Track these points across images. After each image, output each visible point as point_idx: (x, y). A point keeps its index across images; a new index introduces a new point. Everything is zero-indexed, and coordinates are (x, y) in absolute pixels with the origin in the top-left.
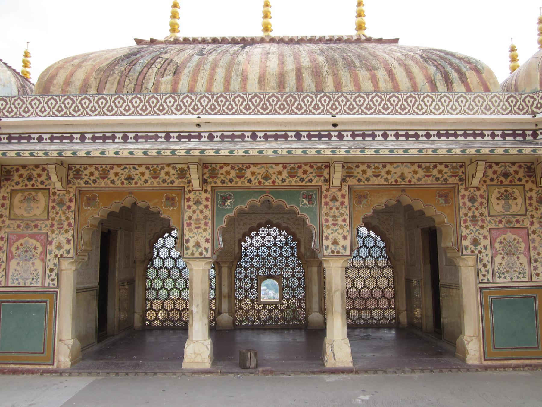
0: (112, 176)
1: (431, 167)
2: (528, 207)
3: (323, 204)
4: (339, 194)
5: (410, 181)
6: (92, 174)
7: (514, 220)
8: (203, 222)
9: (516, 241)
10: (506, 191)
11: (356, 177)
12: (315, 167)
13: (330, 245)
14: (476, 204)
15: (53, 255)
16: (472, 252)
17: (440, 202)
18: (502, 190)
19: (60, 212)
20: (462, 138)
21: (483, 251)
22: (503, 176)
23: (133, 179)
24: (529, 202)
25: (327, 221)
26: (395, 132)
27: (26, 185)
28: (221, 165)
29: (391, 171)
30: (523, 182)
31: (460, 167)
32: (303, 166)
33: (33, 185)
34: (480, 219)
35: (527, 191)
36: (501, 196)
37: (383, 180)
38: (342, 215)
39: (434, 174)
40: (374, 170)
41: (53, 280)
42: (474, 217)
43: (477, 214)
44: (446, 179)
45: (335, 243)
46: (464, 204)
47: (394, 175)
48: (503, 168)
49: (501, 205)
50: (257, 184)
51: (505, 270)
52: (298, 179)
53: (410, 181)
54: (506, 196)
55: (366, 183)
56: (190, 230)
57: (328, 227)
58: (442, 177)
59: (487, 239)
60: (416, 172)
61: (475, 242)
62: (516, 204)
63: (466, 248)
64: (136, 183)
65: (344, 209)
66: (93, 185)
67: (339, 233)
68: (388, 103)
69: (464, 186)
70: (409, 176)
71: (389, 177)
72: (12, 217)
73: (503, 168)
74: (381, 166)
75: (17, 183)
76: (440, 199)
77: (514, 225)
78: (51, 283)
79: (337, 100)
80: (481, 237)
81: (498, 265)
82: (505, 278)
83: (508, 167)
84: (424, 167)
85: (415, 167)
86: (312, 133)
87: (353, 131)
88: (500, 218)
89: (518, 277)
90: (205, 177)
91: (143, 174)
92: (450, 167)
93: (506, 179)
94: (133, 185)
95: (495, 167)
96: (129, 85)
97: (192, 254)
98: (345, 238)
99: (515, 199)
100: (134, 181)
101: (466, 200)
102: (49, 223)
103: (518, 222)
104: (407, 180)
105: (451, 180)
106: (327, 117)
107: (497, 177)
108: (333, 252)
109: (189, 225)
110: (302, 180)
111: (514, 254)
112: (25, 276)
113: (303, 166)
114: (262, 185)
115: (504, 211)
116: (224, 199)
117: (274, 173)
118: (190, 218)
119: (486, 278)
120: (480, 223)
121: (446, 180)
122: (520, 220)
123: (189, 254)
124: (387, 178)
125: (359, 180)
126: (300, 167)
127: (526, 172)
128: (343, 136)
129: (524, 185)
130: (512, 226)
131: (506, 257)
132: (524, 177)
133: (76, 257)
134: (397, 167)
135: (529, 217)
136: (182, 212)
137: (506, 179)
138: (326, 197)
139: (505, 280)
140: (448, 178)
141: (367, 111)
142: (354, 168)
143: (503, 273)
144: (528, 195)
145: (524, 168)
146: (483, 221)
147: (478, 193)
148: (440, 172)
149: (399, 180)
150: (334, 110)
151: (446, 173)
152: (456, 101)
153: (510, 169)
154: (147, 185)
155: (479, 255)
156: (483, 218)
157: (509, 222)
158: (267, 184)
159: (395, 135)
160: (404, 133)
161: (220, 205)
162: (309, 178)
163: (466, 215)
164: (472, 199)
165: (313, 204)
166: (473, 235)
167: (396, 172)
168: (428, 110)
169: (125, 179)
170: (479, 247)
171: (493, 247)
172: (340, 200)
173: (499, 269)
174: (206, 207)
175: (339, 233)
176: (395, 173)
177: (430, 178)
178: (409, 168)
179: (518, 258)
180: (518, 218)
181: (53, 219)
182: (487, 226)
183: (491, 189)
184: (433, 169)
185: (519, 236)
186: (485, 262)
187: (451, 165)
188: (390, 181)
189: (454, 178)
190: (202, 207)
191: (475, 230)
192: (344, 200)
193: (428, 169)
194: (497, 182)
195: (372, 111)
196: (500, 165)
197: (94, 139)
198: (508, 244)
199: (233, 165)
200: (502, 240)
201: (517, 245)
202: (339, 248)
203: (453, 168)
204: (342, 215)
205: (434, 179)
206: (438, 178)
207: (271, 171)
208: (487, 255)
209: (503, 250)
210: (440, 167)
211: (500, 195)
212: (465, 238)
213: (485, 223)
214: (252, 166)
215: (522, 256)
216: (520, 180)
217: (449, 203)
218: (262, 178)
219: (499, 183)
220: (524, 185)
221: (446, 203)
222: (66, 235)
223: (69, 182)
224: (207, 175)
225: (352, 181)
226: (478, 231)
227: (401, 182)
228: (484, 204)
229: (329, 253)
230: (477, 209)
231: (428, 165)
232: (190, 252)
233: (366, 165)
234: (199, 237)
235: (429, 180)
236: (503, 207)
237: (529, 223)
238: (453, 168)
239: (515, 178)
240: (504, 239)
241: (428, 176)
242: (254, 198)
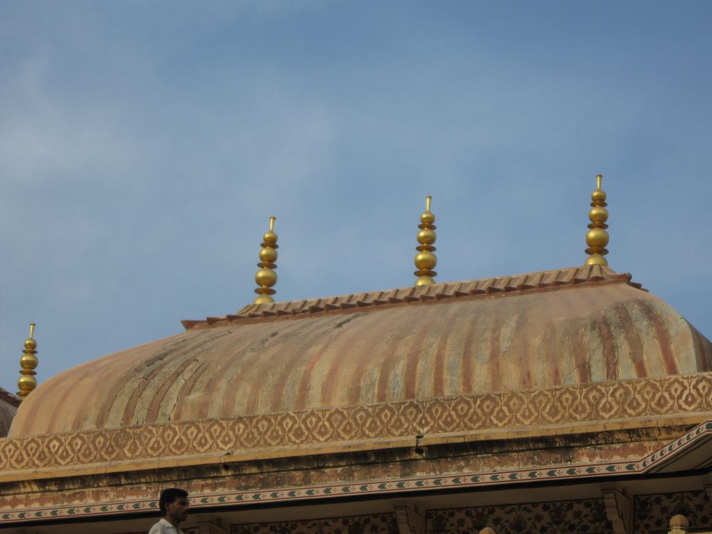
1: (564, 508)
28: (256, 525)
32: (373, 520)
39: (567, 519)
47: (505, 524)
48: (678, 501)
58: (579, 523)
73: (678, 501)
83: (686, 500)
84: (552, 509)
92: (593, 506)
113: (373, 520)
126: (367, 521)
140: (589, 524)
141: (472, 425)
148: (577, 515)
150: (422, 426)
151: (586, 516)
168: (567, 414)
178: (529, 511)
184: (566, 511)
196: (674, 497)
199: (273, 525)
205: (566, 527)
214: (299, 524)
239: (697, 517)
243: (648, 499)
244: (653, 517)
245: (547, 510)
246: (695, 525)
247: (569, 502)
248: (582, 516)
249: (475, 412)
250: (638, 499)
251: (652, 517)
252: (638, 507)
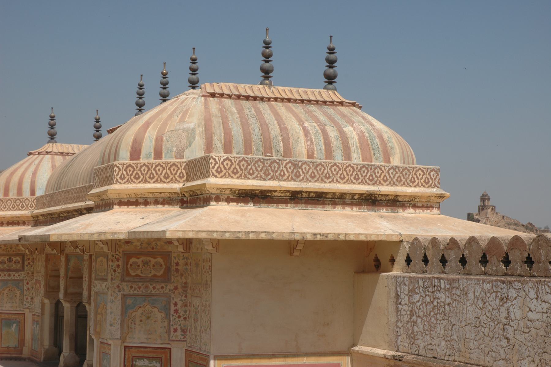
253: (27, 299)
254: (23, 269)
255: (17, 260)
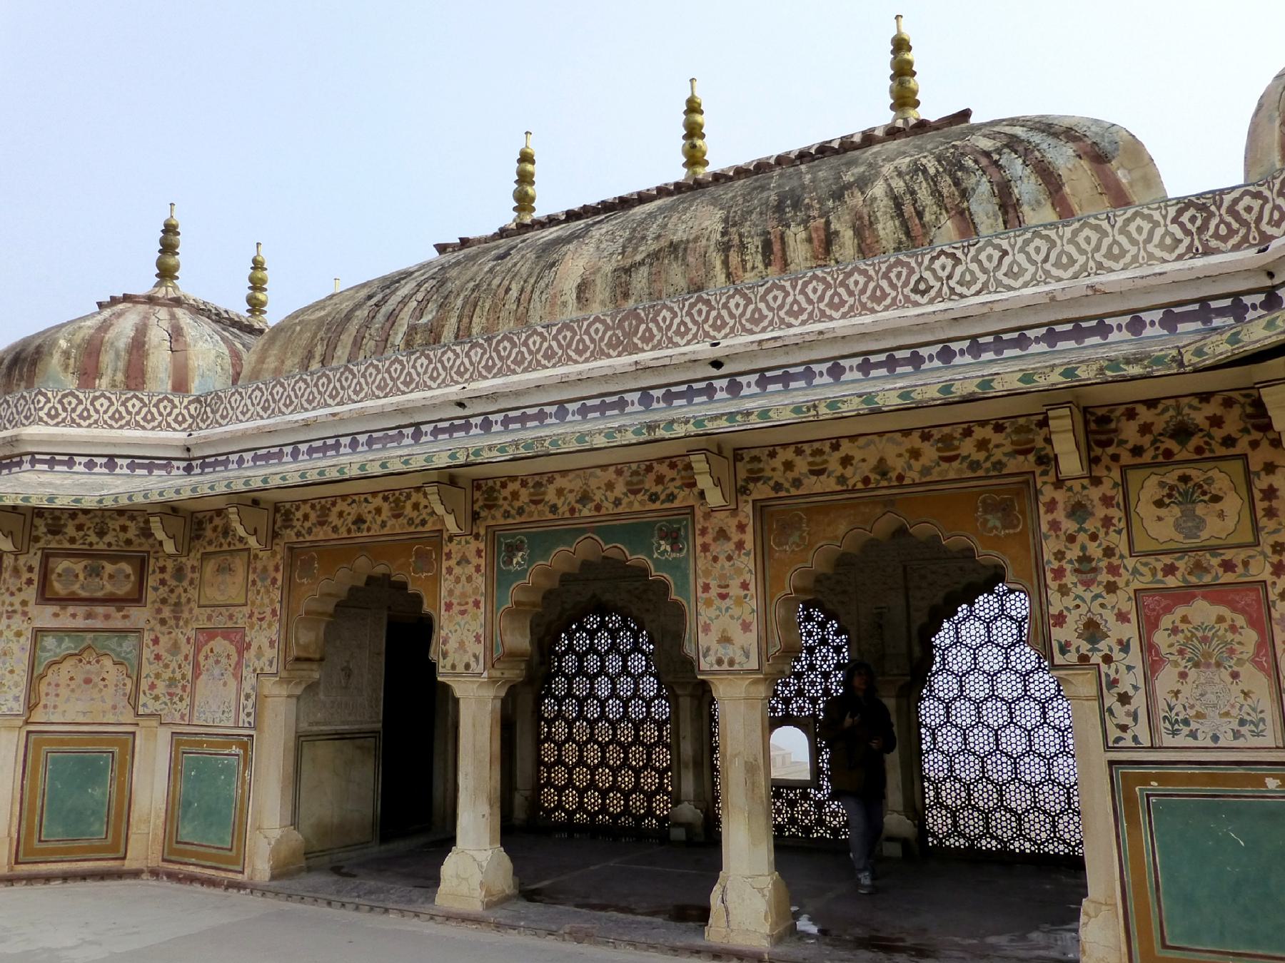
0: (333, 518)
1: (957, 435)
2: (1263, 522)
3: (699, 548)
4: (733, 523)
5: (900, 478)
6: (306, 517)
7: (1215, 562)
8: (471, 600)
9: (1225, 626)
10: (1185, 479)
11: (770, 479)
12: (680, 467)
13: (715, 646)
14: (1090, 525)
15: (251, 669)
16: (1084, 659)
17: (990, 524)
18: (1172, 477)
19: (262, 590)
20: (1043, 347)
21: (1117, 655)
22: (1171, 437)
23: (365, 522)
24: (1266, 504)
25: (706, 588)
26: (859, 360)
27: (221, 545)
29: (852, 458)
30: (1242, 446)
31: (1025, 424)
33: (229, 544)
34: (1103, 564)
35: (1257, 474)
36: (1170, 496)
37: (832, 481)
38: (739, 571)
39: (965, 453)
40: (811, 459)
41: (249, 715)
42: (1085, 558)
43: (1094, 550)
44: (1000, 462)
45: (725, 640)
46: (1055, 525)
47: (861, 464)
48: (1171, 412)
49: (1171, 521)
50: (567, 515)
51: (1192, 713)
52: (646, 497)
53: (900, 478)
54: (1186, 495)
55: (793, 492)
56: (451, 619)
57: (709, 603)
58: (987, 459)
59: (1129, 621)
60: (915, 454)
61: (1092, 631)
62: (1221, 515)
63: (1064, 649)
64: (369, 529)
65: (744, 558)
66: (308, 538)
67: (732, 617)
68: (841, 290)
69: (1051, 477)
70: (898, 465)
71: (849, 472)
72: (202, 603)
73: (1171, 412)
74: (827, 449)
75: (210, 543)
76: (989, 517)
77: (1217, 577)
78: (247, 720)
79: (725, 306)
80: (1109, 616)
81: (1169, 697)
82: (1193, 735)
83: (1186, 410)
84: (936, 437)
85: (915, 441)
86: (674, 389)
87: (762, 371)
88: (1167, 560)
89: (1237, 735)
90: (476, 508)
91: (378, 511)
92: (1008, 430)
93: (1183, 443)
94: (365, 534)
95: (1145, 415)
96: (370, 345)
97: (453, 667)
98: (746, 627)
99: (1216, 499)
100: (365, 526)
101: (1060, 514)
102: (246, 610)
103: (1228, 566)
104: (893, 475)
105: (1013, 465)
106: (702, 349)
107: (1153, 443)
108: (720, 662)
109: (449, 606)
110: (654, 498)
111: (1218, 665)
112: (214, 708)
114: (577, 515)
115: (1180, 538)
116: (512, 549)
117: (599, 488)
118: (451, 592)
119: (1128, 736)
120: (1104, 577)
121: (999, 465)
122: (1238, 561)
123: (448, 666)
124: (842, 476)
125: (778, 487)
126: (649, 469)
127: (1250, 416)
128: (740, 386)
129: (1244, 457)
130: (1207, 579)
131: (1193, 673)
132: (1245, 431)
133: (284, 674)
134: (868, 445)
135: (1269, 551)
136: (436, 580)
137: (1183, 443)
138: (704, 532)
139: (1190, 742)
141: (792, 320)
142: (764, 458)
143: (1186, 722)
144: (1262, 483)
145: (1243, 406)
146: (1113, 570)
147: (1095, 493)
148: (983, 445)
149: (873, 476)
150: (718, 329)
151: (997, 446)
152: (1022, 250)
153: (1194, 414)
154: (385, 531)
155: (1104, 668)
156: (1115, 561)
157: (1199, 568)
158: (586, 512)
159: (859, 367)
160: (883, 357)
161: (504, 563)
162: (668, 492)
163: (1060, 555)
164: (1079, 511)
165: (681, 550)
166: (1084, 609)
167: (866, 457)
169: (354, 523)
170: (1103, 645)
171: (1148, 648)
172: (736, 537)
173: (1171, 709)
174: (478, 569)
175: (732, 617)
176: (864, 460)
177: (955, 464)
179: (1235, 675)
180: (1229, 554)
181: (253, 603)
182: (1127, 584)
183: (1133, 476)
184: (961, 440)
185: (1234, 610)
186: (1125, 686)
187: (1013, 423)
188: (851, 483)
189: (1021, 458)
190: (470, 569)
191: (1088, 596)
192: (744, 537)
193: (947, 441)
194: (1155, 457)
195: (805, 316)
196: (1160, 407)
197: (311, 451)
198: (1199, 634)
200: (1178, 623)
201: (1230, 636)
202: (733, 652)
203: (1019, 430)
204: (739, 571)
205: (965, 465)
206: (978, 462)
207: (593, 483)
208: (1129, 668)
209: (1181, 652)
210: (979, 433)
211: (1166, 491)
212: (1060, 620)
213: (1120, 575)
215: (1247, 670)
216: (1229, 441)
217: (1015, 527)
218: (577, 502)
219: (1161, 459)
220: (1244, 457)
221: (1004, 527)
222: (267, 633)
223: (275, 535)
224: (481, 503)
225: (761, 491)
226: (1100, 600)
227: (878, 482)
228: (1115, 521)
229: (712, 665)
230: (1094, 537)
231: (946, 430)
232: (449, 662)
233: (792, 448)
234: (465, 632)
235: (952, 471)
236: (1177, 526)
237: (1269, 569)
238: (1019, 430)
239: (1212, 438)
240: (1185, 619)
241: (949, 460)
242: (564, 544)
243: (1112, 411)
244: (1126, 442)
245: (928, 440)
246: (1212, 451)
247: (965, 426)
248: (991, 446)
249: (795, 301)
250: (1092, 414)
251: (1122, 442)
252: (1093, 426)
253: (153, 686)
254: (136, 598)
255: (121, 571)
